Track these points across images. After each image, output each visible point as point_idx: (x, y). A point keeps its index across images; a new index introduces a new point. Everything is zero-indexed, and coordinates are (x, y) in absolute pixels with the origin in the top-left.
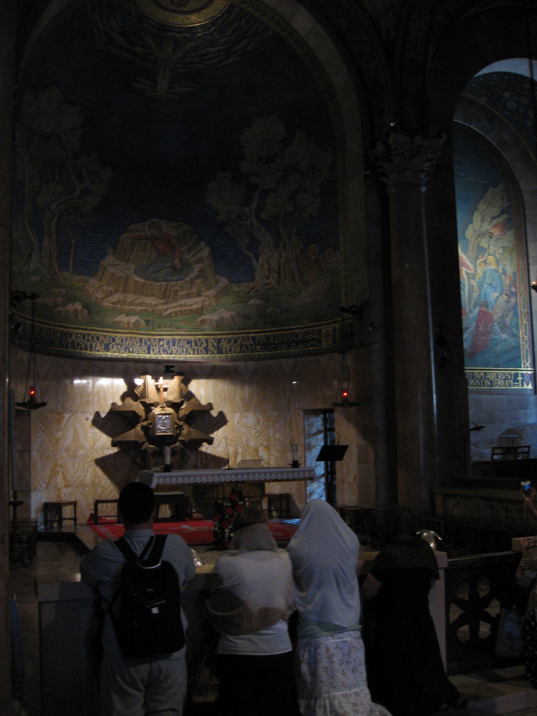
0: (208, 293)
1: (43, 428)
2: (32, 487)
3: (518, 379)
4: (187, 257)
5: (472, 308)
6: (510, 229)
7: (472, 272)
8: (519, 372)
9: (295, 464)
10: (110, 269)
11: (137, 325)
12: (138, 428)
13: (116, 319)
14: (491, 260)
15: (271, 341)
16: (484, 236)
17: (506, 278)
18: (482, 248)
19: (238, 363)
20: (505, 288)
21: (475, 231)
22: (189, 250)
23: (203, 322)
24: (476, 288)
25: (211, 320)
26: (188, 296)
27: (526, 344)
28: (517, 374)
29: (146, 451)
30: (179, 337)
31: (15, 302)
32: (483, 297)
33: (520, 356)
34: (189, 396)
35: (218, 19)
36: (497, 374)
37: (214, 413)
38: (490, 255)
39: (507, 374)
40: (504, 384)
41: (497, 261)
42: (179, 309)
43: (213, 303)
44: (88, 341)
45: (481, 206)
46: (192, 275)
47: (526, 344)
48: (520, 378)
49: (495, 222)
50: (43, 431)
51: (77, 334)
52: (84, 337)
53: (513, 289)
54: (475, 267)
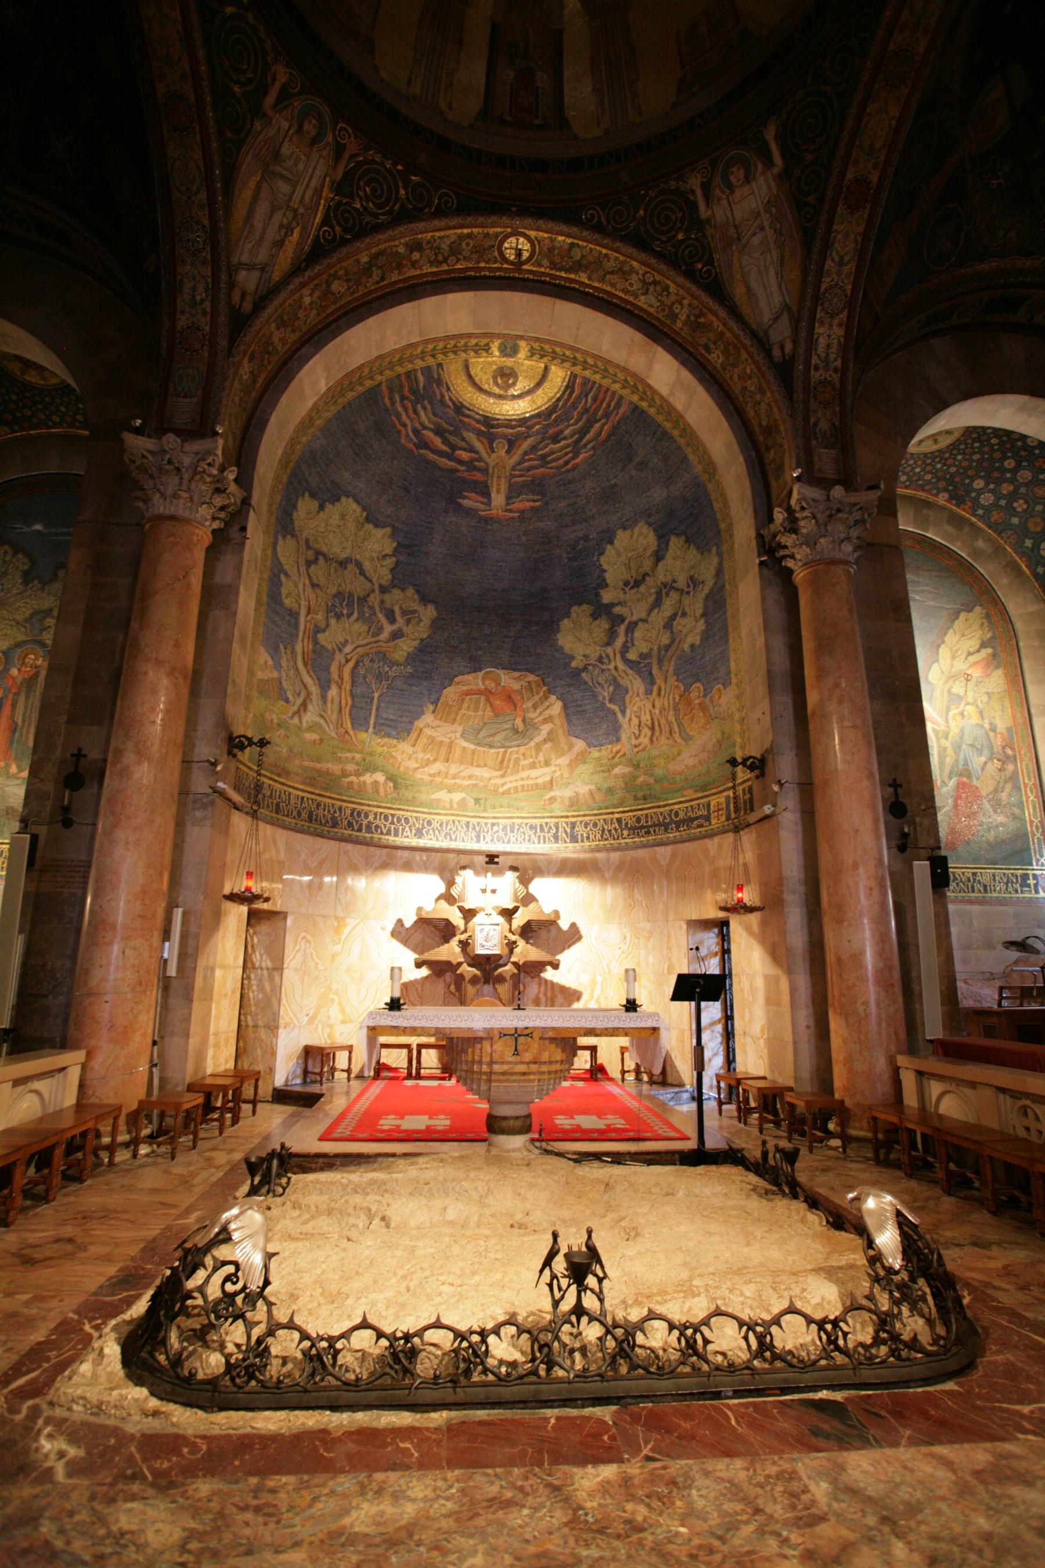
0: (560, 761)
1: (309, 937)
2: (282, 1022)
4: (532, 715)
6: (996, 668)
7: (943, 728)
9: (631, 1006)
10: (428, 732)
11: (462, 804)
12: (454, 942)
13: (433, 797)
15: (643, 822)
19: (598, 855)
22: (535, 707)
23: (552, 800)
25: (562, 798)
26: (533, 766)
29: (461, 975)
30: (520, 821)
31: (236, 751)
32: (961, 763)
33: (1029, 848)
34: (528, 899)
35: (559, 400)
37: (564, 924)
38: (968, 704)
41: (981, 713)
42: (520, 783)
43: (566, 775)
44: (392, 823)
45: (951, 638)
46: (538, 739)
48: (1032, 882)
49: (972, 659)
50: (308, 942)
51: (376, 814)
52: (386, 818)
53: (1009, 752)
54: (947, 721)
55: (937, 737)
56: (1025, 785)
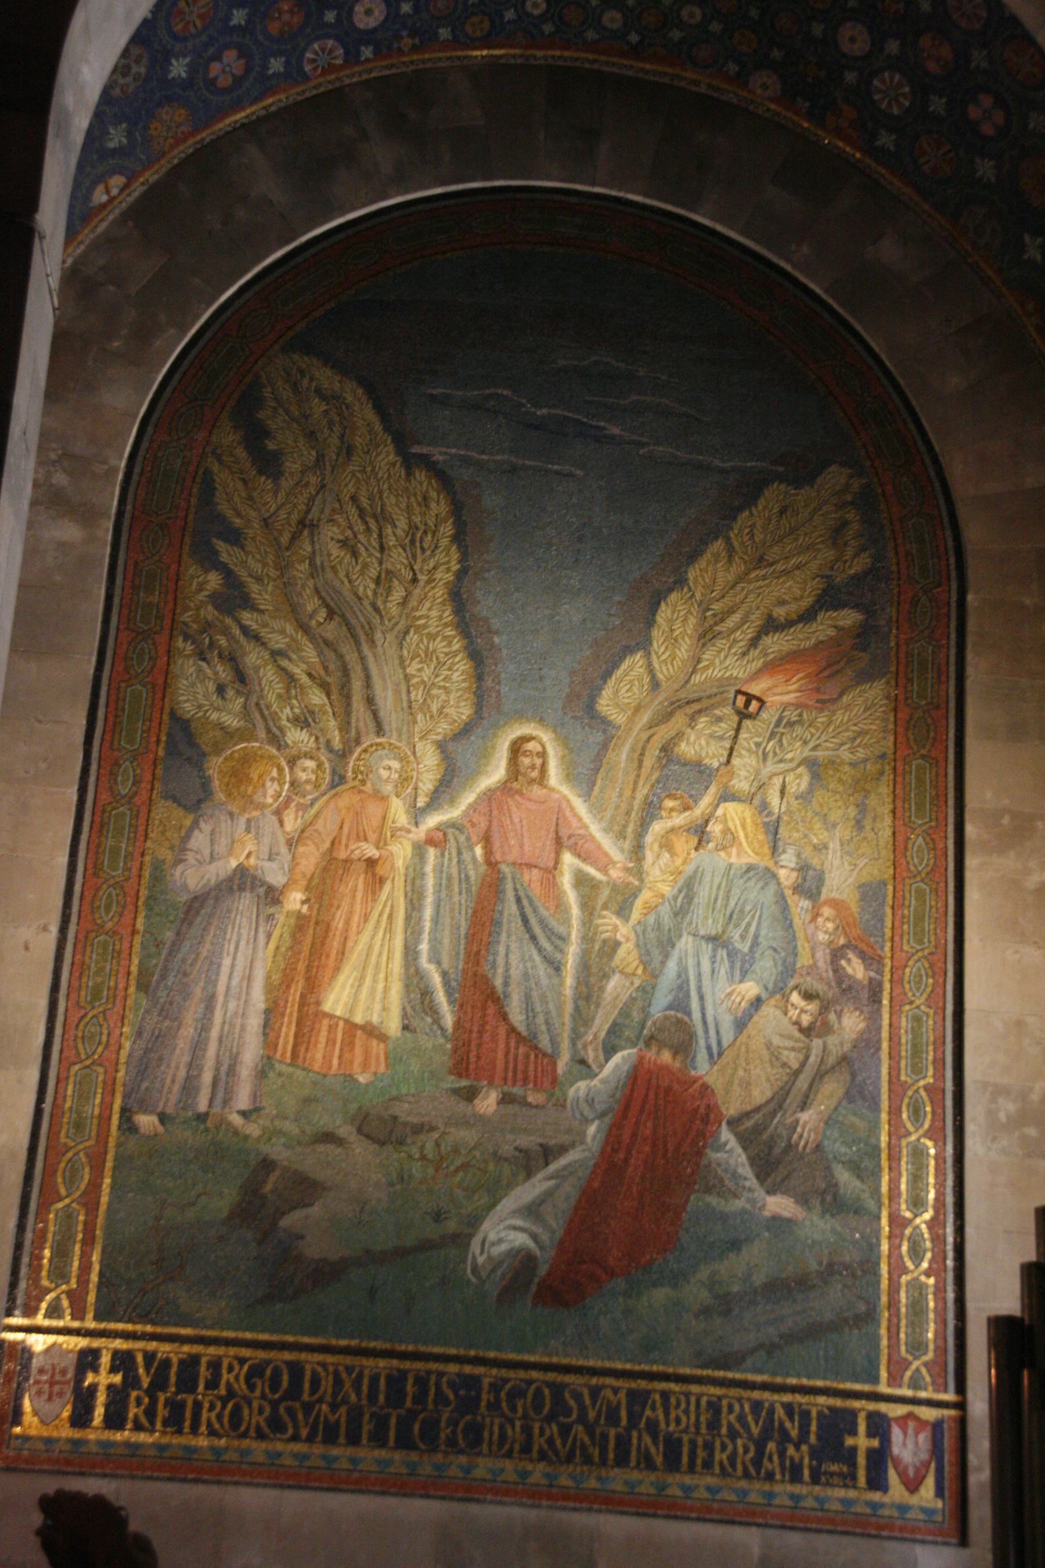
3: (849, 1441)
5: (590, 1055)
6: (865, 677)
7: (615, 874)
8: (857, 1404)
14: (735, 824)
16: (707, 709)
17: (816, 916)
18: (685, 764)
20: (804, 960)
21: (655, 685)
24: (627, 954)
27: (916, 1254)
28: (854, 1414)
36: (714, 1407)
38: (727, 796)
39: (780, 1412)
40: (757, 1462)
41: (773, 830)
47: (916, 1254)
48: (862, 1442)
49: (776, 644)
53: (856, 969)
55: (588, 907)
56: (897, 1088)
